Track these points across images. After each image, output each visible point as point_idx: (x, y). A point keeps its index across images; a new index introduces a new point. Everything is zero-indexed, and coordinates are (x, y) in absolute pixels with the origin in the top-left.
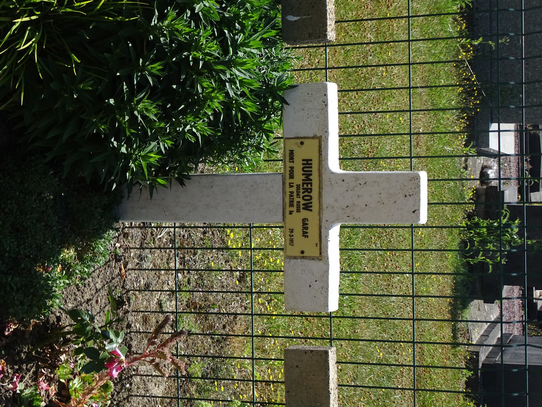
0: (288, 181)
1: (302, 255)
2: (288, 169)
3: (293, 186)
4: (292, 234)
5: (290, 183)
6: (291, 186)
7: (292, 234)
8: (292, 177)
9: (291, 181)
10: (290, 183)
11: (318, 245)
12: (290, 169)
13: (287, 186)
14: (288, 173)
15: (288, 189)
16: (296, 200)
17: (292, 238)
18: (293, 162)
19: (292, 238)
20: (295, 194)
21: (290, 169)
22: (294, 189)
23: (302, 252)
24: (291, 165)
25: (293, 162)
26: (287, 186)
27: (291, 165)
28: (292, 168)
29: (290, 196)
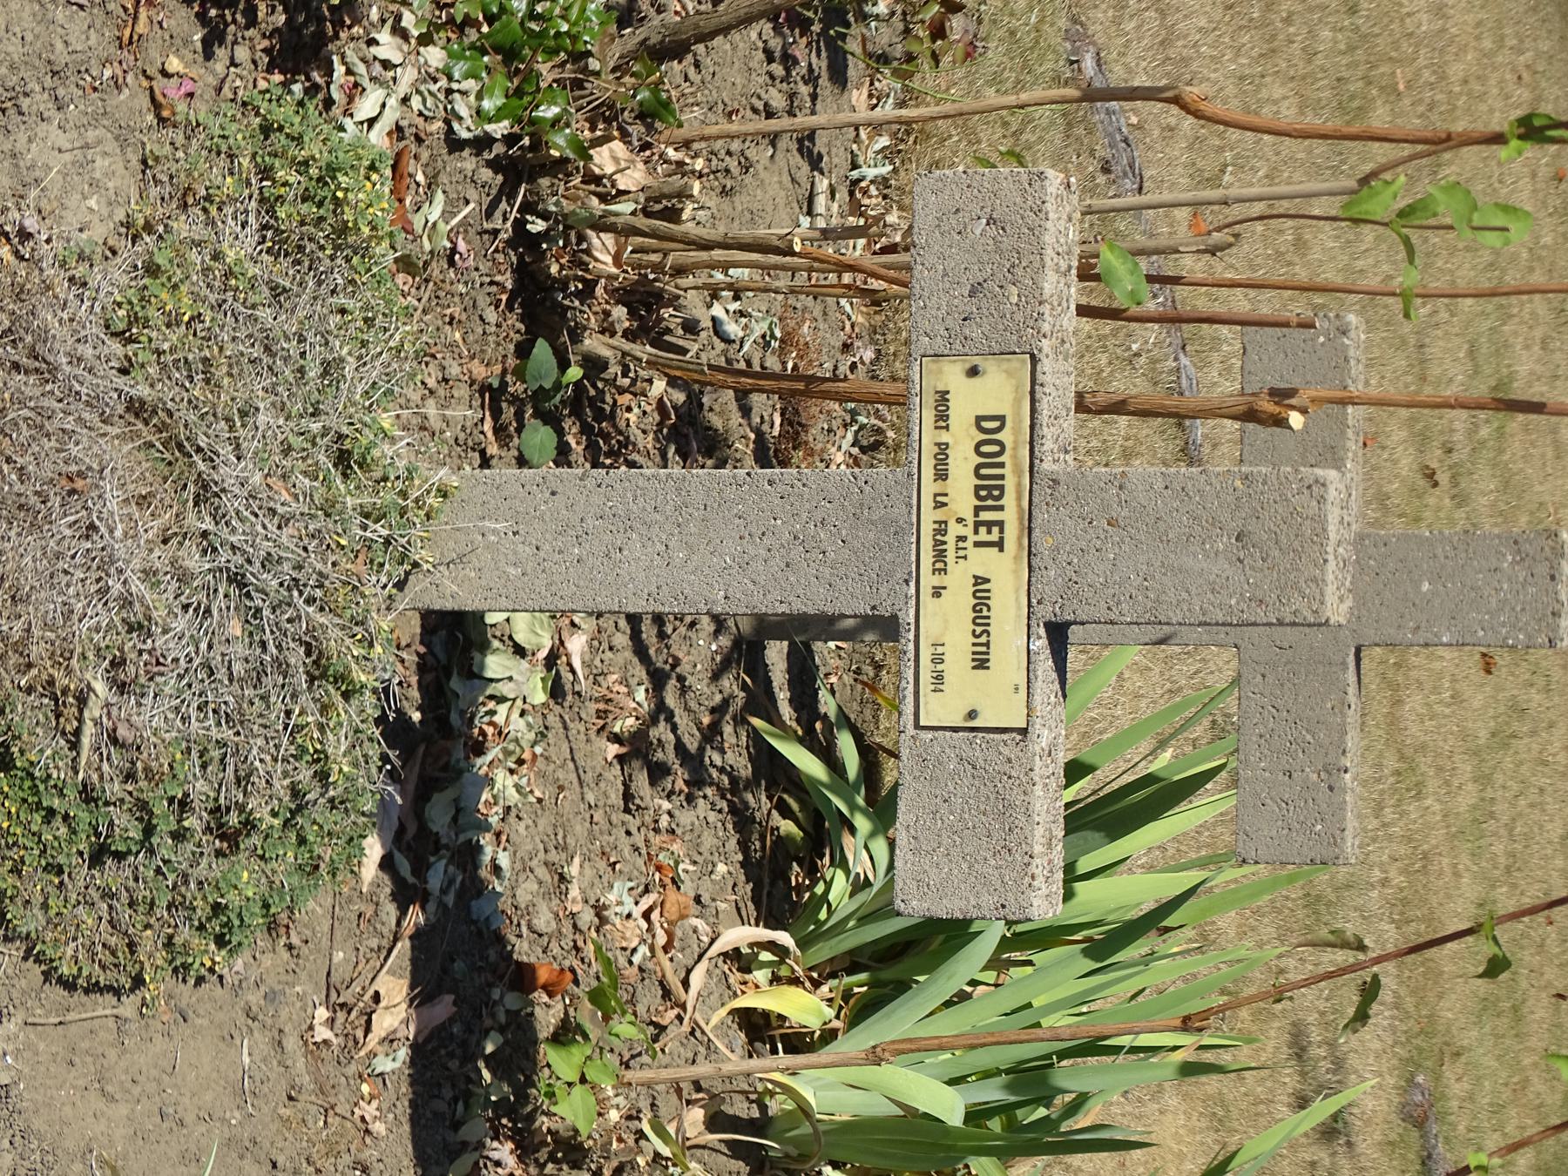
0: (929, 487)
2: (928, 450)
3: (945, 504)
5: (936, 495)
6: (940, 505)
8: (941, 475)
10: (936, 495)
12: (936, 450)
15: (929, 517)
17: (940, 667)
18: (947, 428)
19: (940, 667)
21: (936, 450)
24: (944, 437)
25: (947, 428)
27: (944, 437)
28: (943, 448)
29: (937, 532)
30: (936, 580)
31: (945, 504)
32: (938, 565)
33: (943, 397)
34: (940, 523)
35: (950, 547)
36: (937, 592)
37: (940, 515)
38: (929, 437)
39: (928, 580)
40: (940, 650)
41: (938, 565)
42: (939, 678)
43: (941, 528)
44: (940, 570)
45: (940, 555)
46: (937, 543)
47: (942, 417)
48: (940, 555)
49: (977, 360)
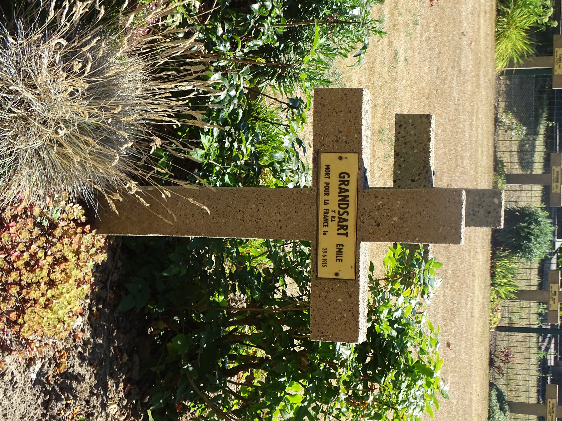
0: (322, 197)
1: (335, 277)
3: (328, 204)
4: (325, 254)
8: (327, 194)
9: (326, 197)
11: (353, 267)
12: (325, 185)
15: (322, 207)
17: (325, 258)
18: (329, 178)
20: (330, 211)
21: (325, 185)
23: (337, 274)
24: (327, 180)
25: (329, 178)
26: (321, 203)
27: (327, 180)
28: (327, 184)
30: (326, 229)
31: (328, 204)
33: (328, 167)
34: (326, 210)
35: (330, 218)
36: (325, 233)
37: (326, 207)
38: (323, 180)
39: (322, 229)
40: (325, 254)
42: (325, 261)
43: (327, 211)
44: (326, 226)
45: (326, 221)
46: (325, 216)
47: (327, 174)
48: (326, 221)
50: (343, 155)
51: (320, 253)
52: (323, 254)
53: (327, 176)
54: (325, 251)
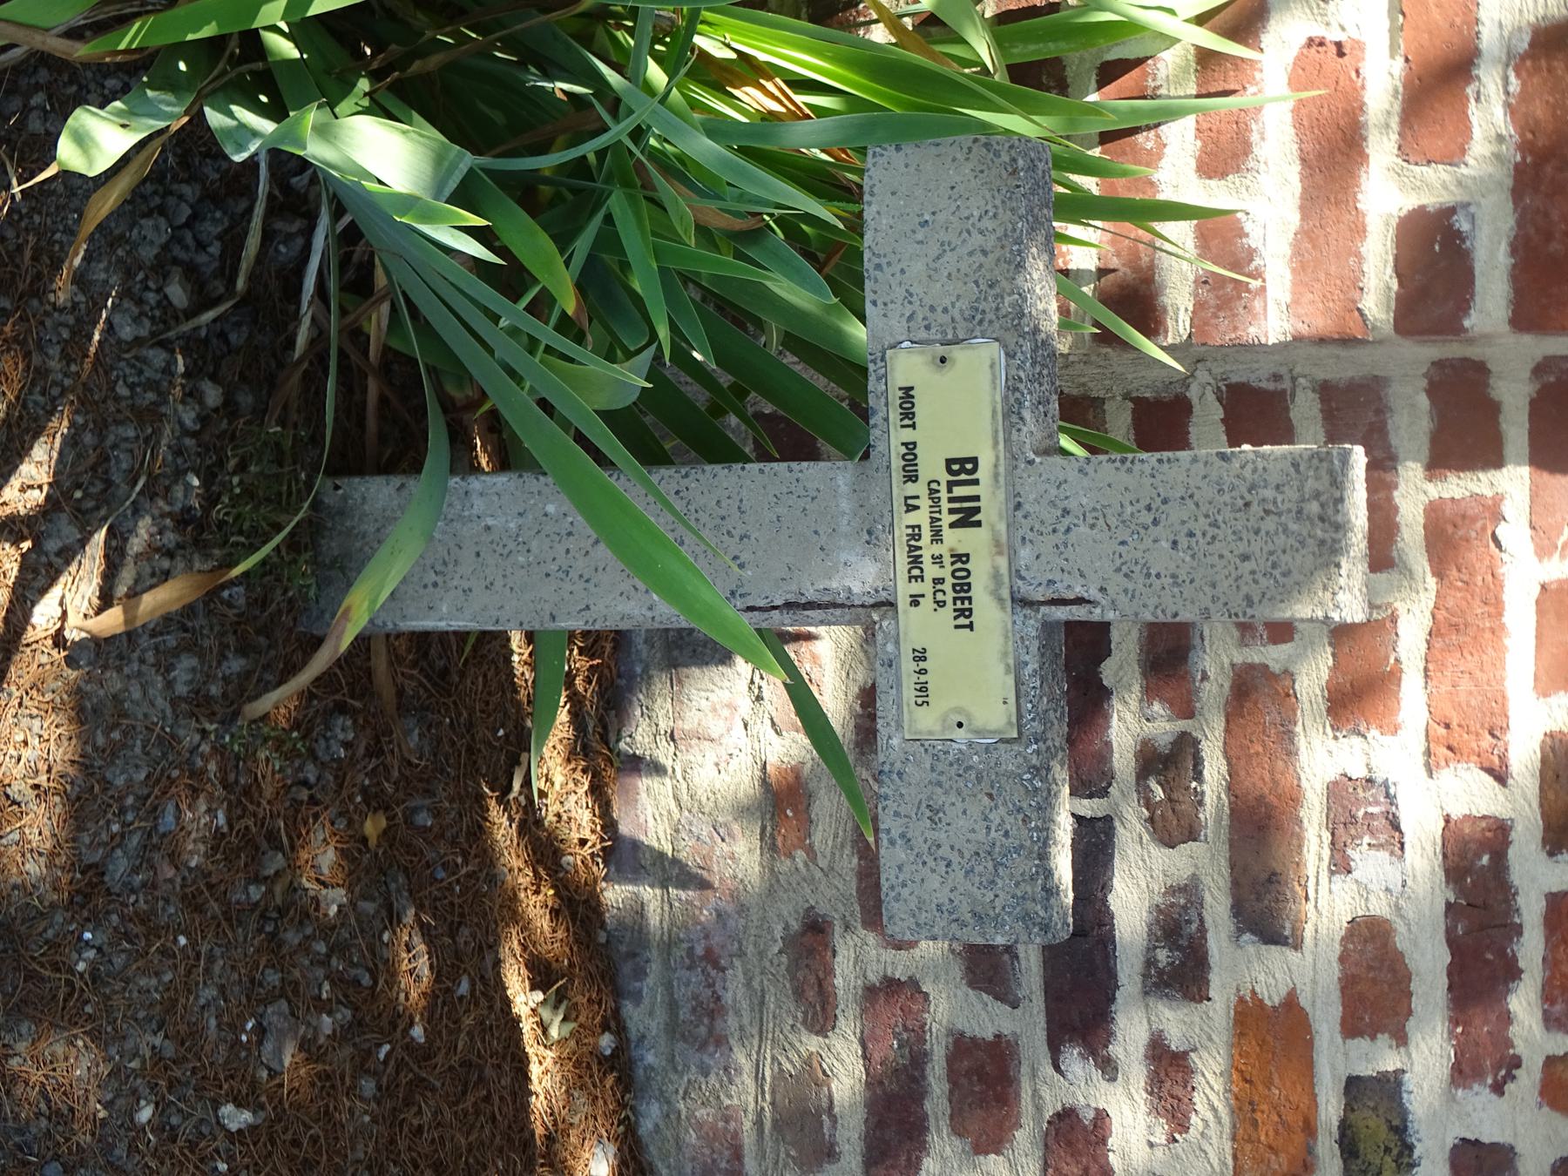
0: (901, 489)
5: (906, 498)
7: (922, 665)
8: (912, 477)
9: (911, 489)
13: (898, 505)
14: (896, 464)
16: (928, 551)
17: (923, 678)
18: (913, 426)
19: (923, 678)
21: (903, 450)
22: (922, 517)
24: (908, 436)
25: (913, 426)
26: (898, 505)
27: (908, 436)
28: (911, 446)
30: (916, 588)
32: (916, 572)
33: (907, 391)
34: (913, 527)
36: (915, 601)
38: (899, 436)
41: (916, 572)
42: (923, 689)
44: (916, 578)
45: (916, 561)
46: (912, 549)
47: (908, 414)
48: (916, 561)
49: (940, 350)
50: (956, 352)
51: (908, 665)
52: (913, 666)
53: (907, 422)
54: (920, 656)
